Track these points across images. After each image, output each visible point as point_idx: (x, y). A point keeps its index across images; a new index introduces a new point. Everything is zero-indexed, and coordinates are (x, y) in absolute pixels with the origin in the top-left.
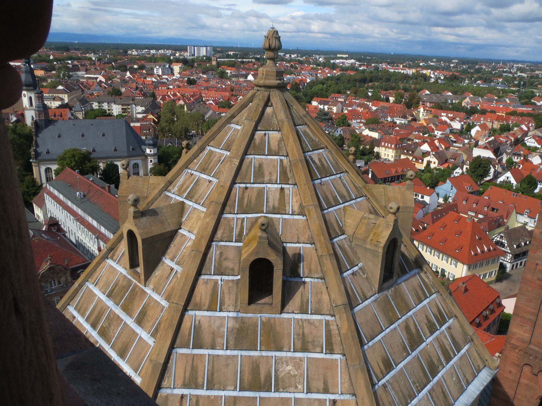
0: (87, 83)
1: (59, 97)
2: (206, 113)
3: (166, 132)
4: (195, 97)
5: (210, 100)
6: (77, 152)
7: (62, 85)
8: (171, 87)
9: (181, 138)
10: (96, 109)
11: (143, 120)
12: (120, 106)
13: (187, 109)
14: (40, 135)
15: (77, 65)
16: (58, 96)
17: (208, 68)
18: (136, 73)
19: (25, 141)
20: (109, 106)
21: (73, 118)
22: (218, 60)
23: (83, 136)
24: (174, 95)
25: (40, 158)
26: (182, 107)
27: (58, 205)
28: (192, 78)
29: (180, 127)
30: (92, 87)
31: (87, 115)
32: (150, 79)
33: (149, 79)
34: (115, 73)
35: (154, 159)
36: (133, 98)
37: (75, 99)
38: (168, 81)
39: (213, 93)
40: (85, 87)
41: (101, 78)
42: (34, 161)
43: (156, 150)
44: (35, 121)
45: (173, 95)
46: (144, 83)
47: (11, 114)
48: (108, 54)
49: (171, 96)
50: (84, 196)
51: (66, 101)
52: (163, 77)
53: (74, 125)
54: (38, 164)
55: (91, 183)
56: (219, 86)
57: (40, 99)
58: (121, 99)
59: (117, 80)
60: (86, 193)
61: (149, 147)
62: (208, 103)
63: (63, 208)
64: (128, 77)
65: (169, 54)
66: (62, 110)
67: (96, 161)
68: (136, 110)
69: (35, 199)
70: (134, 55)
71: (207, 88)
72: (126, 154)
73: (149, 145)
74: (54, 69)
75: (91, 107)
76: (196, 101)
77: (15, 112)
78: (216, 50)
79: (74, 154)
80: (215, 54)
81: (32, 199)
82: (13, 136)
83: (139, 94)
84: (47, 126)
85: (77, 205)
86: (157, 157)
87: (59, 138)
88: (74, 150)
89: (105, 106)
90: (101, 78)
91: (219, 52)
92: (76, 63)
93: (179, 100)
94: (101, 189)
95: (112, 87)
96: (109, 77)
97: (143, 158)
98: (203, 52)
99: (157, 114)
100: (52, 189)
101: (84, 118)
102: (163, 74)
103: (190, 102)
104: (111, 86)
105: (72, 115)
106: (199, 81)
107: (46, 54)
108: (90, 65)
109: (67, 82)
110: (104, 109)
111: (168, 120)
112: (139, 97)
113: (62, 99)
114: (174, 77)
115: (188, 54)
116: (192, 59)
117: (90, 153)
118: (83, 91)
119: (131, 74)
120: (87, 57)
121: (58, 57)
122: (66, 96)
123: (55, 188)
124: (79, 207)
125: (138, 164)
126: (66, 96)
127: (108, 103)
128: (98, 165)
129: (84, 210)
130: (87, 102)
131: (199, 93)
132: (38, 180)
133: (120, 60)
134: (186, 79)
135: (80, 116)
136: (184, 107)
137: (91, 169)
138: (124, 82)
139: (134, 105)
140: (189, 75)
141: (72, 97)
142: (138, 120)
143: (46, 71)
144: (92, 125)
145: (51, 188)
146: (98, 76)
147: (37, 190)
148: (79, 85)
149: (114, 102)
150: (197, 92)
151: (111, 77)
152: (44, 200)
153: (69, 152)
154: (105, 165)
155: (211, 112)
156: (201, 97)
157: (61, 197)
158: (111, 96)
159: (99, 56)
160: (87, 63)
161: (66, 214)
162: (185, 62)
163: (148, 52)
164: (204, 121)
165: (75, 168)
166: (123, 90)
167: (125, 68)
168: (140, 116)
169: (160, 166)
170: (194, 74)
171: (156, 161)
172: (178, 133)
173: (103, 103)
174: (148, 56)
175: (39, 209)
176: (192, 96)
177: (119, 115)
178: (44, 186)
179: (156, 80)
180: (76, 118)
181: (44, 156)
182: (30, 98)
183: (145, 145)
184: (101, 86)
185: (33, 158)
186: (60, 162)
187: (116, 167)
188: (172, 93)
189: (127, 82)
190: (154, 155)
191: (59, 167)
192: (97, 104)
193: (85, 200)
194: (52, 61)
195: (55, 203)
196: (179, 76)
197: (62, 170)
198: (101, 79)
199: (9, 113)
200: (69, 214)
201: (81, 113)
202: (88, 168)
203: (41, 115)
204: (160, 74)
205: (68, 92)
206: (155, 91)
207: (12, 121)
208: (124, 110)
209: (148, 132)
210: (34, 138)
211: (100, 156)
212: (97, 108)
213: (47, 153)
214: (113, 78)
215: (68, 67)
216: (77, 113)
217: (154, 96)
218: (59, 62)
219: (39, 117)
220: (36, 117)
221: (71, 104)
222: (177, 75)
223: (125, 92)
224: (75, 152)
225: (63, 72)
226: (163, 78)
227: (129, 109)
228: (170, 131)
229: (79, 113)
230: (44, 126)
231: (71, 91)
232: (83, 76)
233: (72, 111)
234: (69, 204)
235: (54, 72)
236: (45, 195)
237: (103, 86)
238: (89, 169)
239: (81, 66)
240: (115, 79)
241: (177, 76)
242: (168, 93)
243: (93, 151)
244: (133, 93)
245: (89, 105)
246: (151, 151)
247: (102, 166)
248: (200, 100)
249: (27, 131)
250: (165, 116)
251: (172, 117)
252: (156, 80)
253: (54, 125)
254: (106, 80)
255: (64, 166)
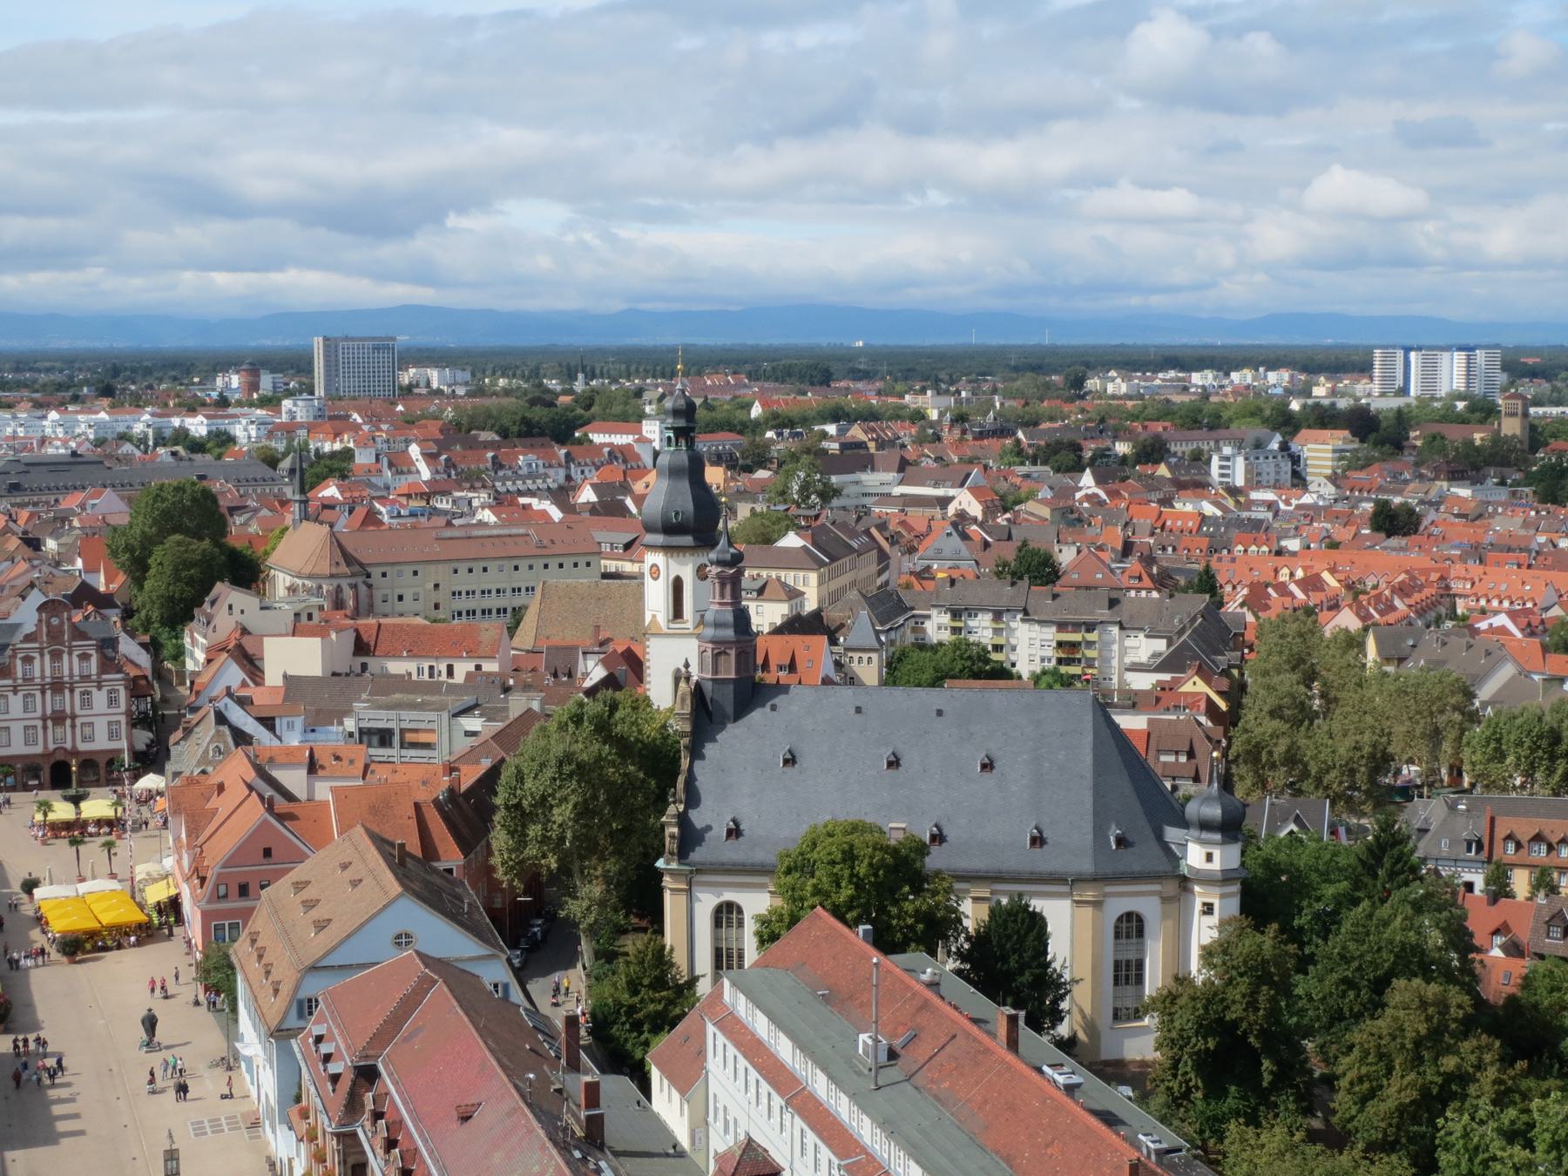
0: (903, 523)
1: (784, 585)
2: (1481, 678)
3: (1273, 766)
4: (1417, 597)
5: (1496, 612)
6: (868, 837)
7: (799, 529)
8: (1293, 545)
9: (1349, 800)
10: (941, 644)
11: (1158, 700)
12: (1051, 634)
13: (1380, 651)
14: (710, 750)
15: (861, 445)
16: (778, 579)
17: (1478, 450)
18: (1123, 480)
19: (641, 775)
20: (997, 631)
21: (837, 679)
22: (1532, 410)
23: (894, 763)
24: (1312, 583)
25: (698, 855)
26: (1354, 643)
27: (765, 1087)
28: (1397, 500)
29: (1349, 742)
30: (926, 542)
31: (894, 671)
32: (1189, 508)
33: (1185, 506)
34: (1027, 476)
35: (1222, 896)
36: (1114, 595)
37: (853, 595)
38: (1276, 514)
39: (1506, 578)
40: (893, 540)
41: (966, 502)
42: (674, 865)
43: (1235, 850)
44: (698, 684)
45: (1306, 585)
46: (1163, 527)
47: (584, 653)
48: (995, 391)
49: (1293, 588)
50: (892, 1055)
51: (810, 605)
52: (1254, 495)
53: (858, 710)
54: (690, 884)
55: (929, 994)
56: (1542, 539)
57: (728, 589)
58: (1055, 597)
59: (1037, 509)
60: (897, 1043)
61: (1205, 835)
62: (1483, 625)
63: (788, 1103)
64: (1088, 498)
65: (1279, 391)
66: (797, 642)
67: (949, 890)
68: (1124, 651)
69: (663, 1043)
70: (1114, 397)
71: (1478, 553)
72: (1086, 866)
73: (1205, 826)
74: (762, 462)
75: (918, 629)
76: (1421, 613)
77: (601, 644)
78: (1516, 368)
79: (852, 847)
80: (1512, 384)
81: (647, 1044)
82: (597, 746)
83: (1140, 578)
84: (742, 709)
85: (853, 1096)
86: (1235, 888)
87: (789, 770)
88: (855, 828)
89: (982, 629)
90: (966, 502)
91: (1533, 373)
92: (857, 432)
93: (1335, 607)
94: (974, 1030)
95: (1016, 543)
96: (1002, 498)
97: (1171, 888)
98: (1452, 375)
99: (1226, 673)
100: (741, 1006)
101: (884, 683)
102: (1255, 481)
103: (1391, 618)
104: (1010, 538)
105: (838, 665)
106: (1432, 515)
107: (735, 397)
108: (920, 441)
109: (817, 517)
110: (978, 644)
111: (1280, 707)
112: (1138, 590)
113: (793, 594)
114: (1307, 499)
115: (1376, 388)
116: (1399, 412)
117: (922, 850)
118: (883, 557)
119: (1100, 481)
120: (905, 407)
121: (782, 409)
122: (813, 577)
123: (757, 1002)
124: (864, 1109)
125: (1140, 919)
126: (813, 577)
127: (998, 616)
128: (955, 911)
129: (889, 1126)
130: (901, 608)
131: (1434, 577)
132: (680, 958)
133: (1052, 419)
134: (1368, 506)
135: (869, 670)
136: (1361, 646)
137: (920, 927)
138: (1070, 518)
139: (1115, 630)
140: (1380, 489)
141: (835, 584)
142: (1134, 702)
143: (729, 468)
144: (940, 713)
145: (742, 998)
146: (951, 492)
147: (671, 1002)
148: (867, 533)
149: (1026, 612)
150: (1426, 572)
151: (1011, 498)
152: (701, 1054)
153: (830, 835)
154: (983, 912)
155: (1507, 671)
156: (1448, 595)
157: (784, 1049)
158: (1013, 584)
159: (959, 402)
160: (907, 433)
161: (797, 1134)
162: (1362, 423)
163: (1179, 380)
164: (1473, 717)
165: (849, 916)
166: (1066, 556)
167: (1072, 456)
168: (1143, 682)
169: (1259, 938)
170: (1406, 482)
171: (1234, 905)
172: (1333, 774)
173: (972, 612)
174: (1177, 399)
175: (676, 1095)
176: (1402, 590)
177: (1044, 672)
178: (704, 988)
179: (1219, 513)
180: (852, 680)
181: (714, 848)
182: (678, 585)
183: (1184, 823)
184: (965, 537)
185: (672, 853)
186: (789, 879)
187: (1037, 924)
188: (1300, 574)
189: (1080, 520)
190: (1226, 878)
191: (779, 902)
192: (946, 619)
193: (894, 1073)
194: (757, 427)
195: (754, 1075)
196: (1329, 490)
197: (794, 920)
198: (965, 506)
199: (574, 649)
200: (811, 1137)
201: (875, 656)
202: (910, 921)
203: (722, 658)
204: (1240, 481)
205: (821, 564)
206: (1214, 565)
207: (588, 684)
208: (1068, 651)
209: (1183, 759)
210: (685, 763)
211: (964, 864)
212: (946, 636)
213: (730, 833)
214: (1019, 502)
215: (825, 452)
216: (856, 656)
217: (1207, 583)
218: (786, 432)
219: (715, 671)
220: (702, 670)
221: (833, 615)
222: (1319, 491)
223: (1076, 566)
224: (856, 839)
225: (802, 475)
226: (1250, 504)
227: (1090, 644)
228: (1292, 759)
229: (865, 656)
230: (729, 709)
231: (833, 559)
232: (885, 490)
233: (835, 649)
234: (820, 1085)
235: (762, 474)
236: (711, 1029)
237: (977, 539)
238: (911, 928)
239: (881, 445)
240: (1030, 506)
241: (1323, 490)
242: (1276, 571)
243: (933, 838)
244: (1112, 571)
245: (911, 623)
246: (1209, 857)
247: (972, 913)
248: (1443, 611)
249: (650, 731)
250: (1269, 688)
251: (1302, 688)
252: (1219, 513)
253: (774, 708)
254: (989, 511)
255: (802, 899)
